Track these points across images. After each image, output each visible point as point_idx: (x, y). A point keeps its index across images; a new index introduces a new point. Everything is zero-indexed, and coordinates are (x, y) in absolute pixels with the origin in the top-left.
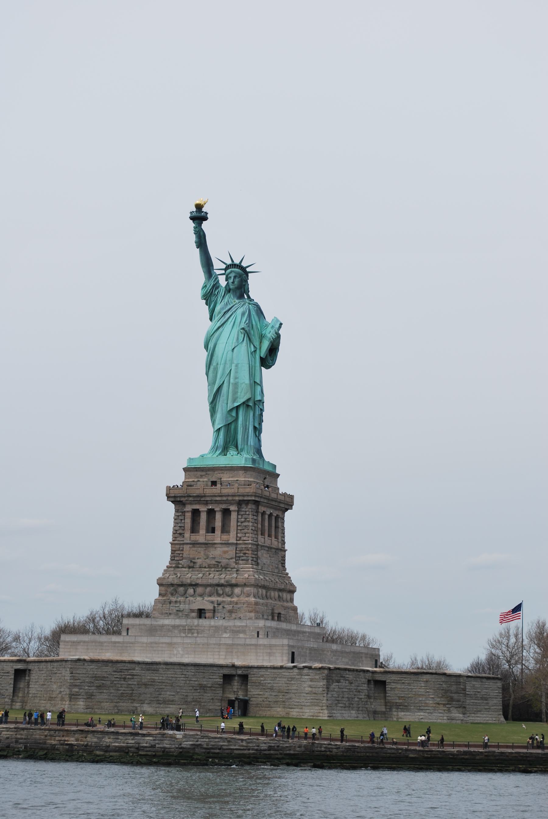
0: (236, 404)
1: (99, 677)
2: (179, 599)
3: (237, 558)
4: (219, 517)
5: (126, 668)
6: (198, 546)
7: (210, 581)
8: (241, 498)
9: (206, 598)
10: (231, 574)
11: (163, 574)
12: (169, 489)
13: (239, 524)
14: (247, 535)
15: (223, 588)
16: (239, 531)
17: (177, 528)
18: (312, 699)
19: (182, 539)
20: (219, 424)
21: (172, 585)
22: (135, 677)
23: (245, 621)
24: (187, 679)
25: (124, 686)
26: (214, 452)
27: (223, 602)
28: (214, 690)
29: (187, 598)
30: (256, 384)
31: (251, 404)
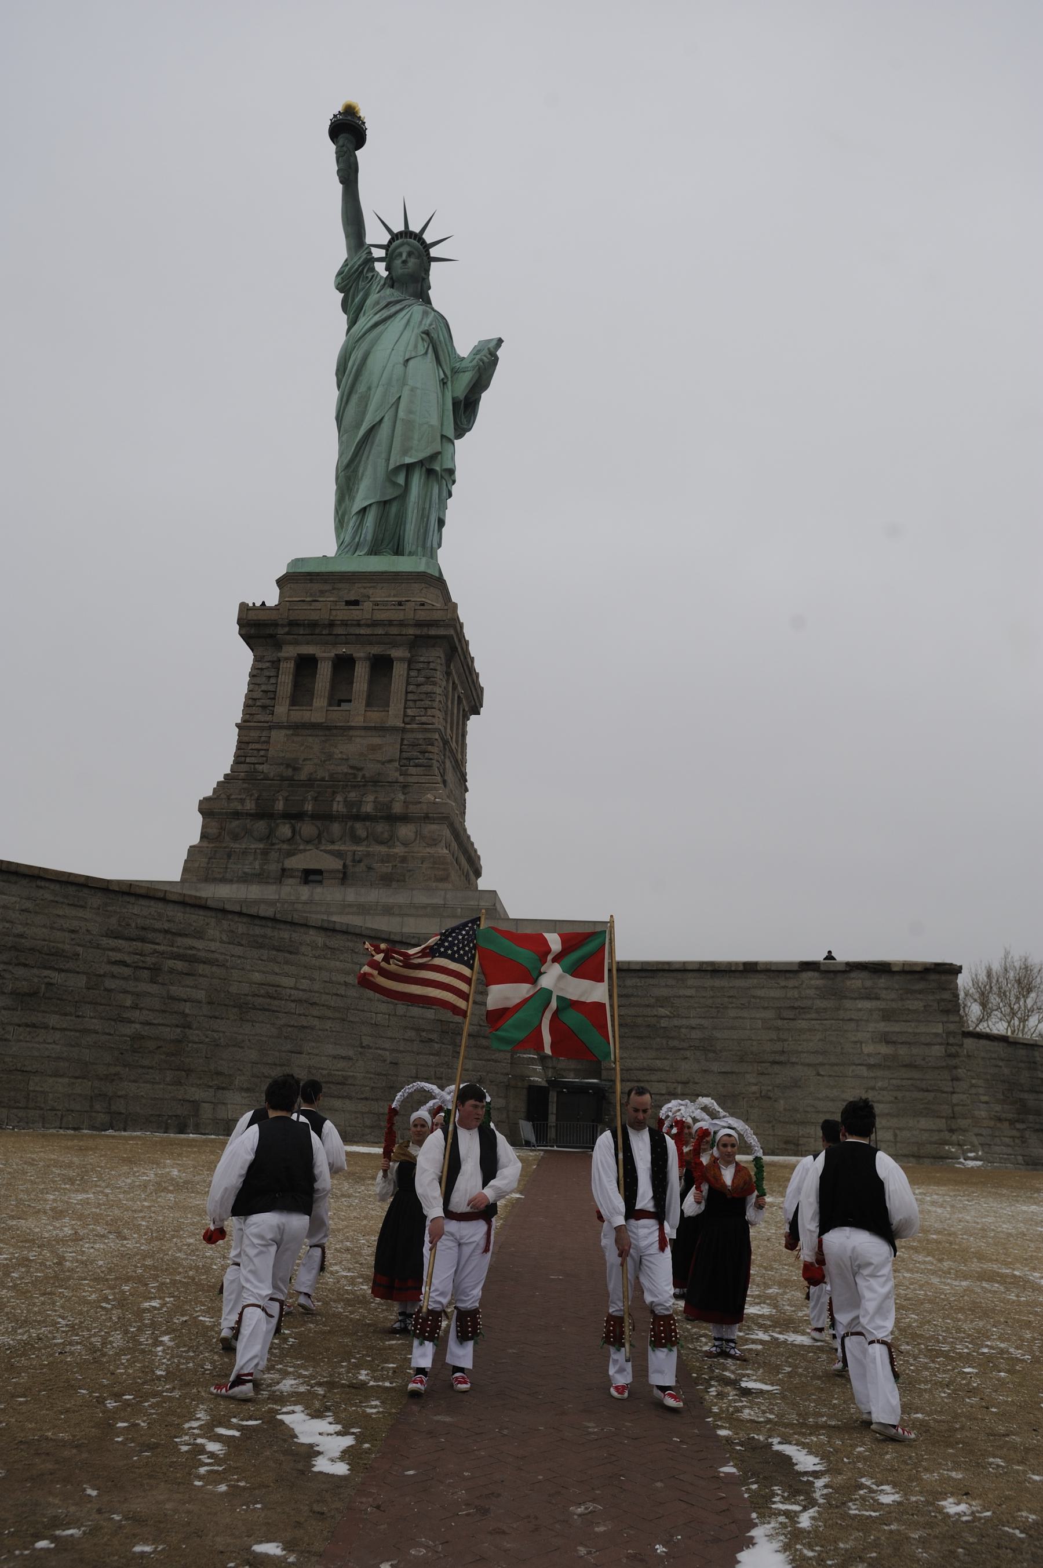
0: (408, 460)
1: (32, 950)
3: (405, 761)
4: (361, 672)
5: (166, 926)
12: (244, 607)
13: (411, 688)
14: (430, 712)
15: (368, 823)
16: (410, 704)
17: (257, 694)
18: (899, 1088)
19: (269, 718)
20: (365, 499)
22: (201, 968)
23: (443, 893)
26: (350, 553)
27: (368, 855)
28: (487, 1048)
30: (444, 440)
31: (438, 468)
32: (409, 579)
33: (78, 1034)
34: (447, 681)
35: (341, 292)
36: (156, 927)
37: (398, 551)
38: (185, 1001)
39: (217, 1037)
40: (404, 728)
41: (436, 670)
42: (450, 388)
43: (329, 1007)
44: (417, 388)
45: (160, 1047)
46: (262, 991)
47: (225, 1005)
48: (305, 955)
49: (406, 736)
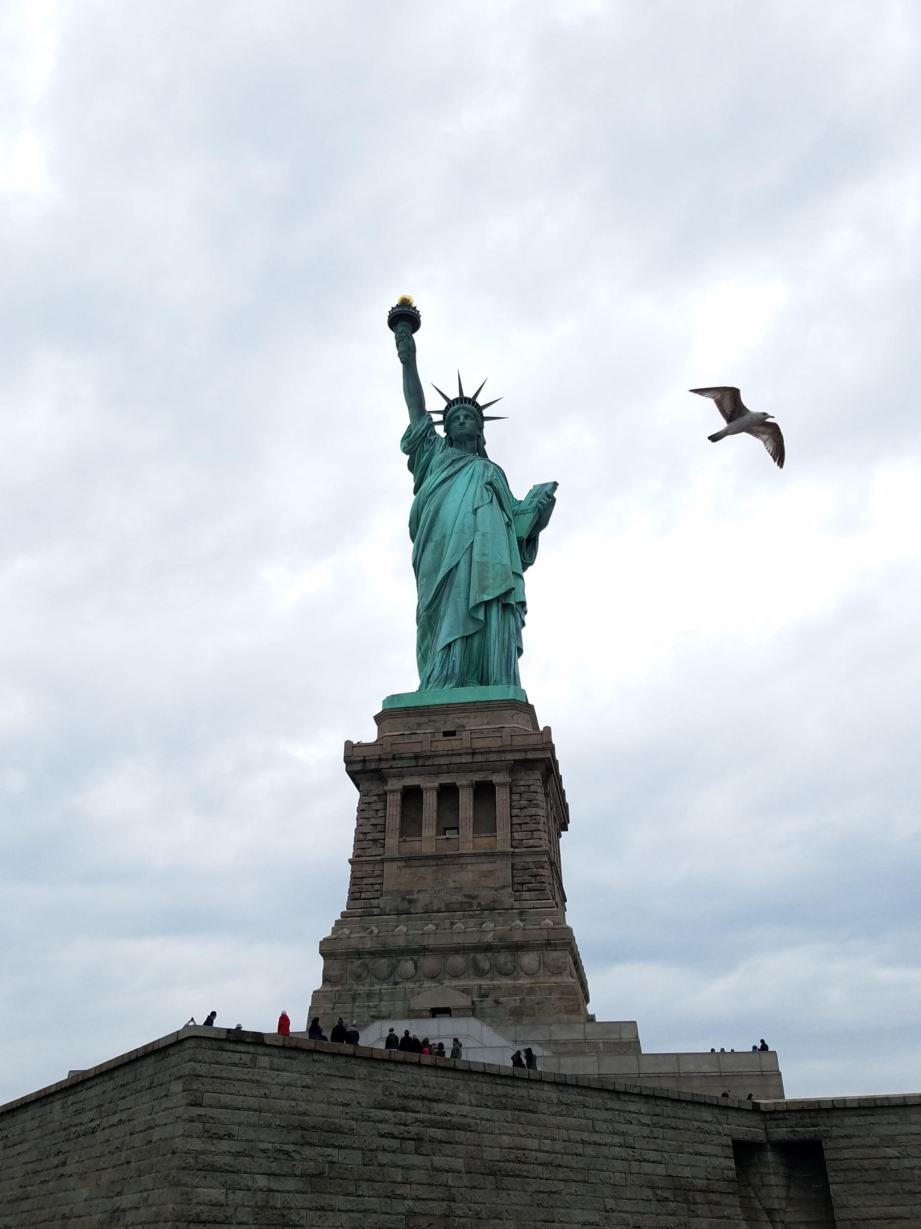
0: (486, 598)
2: (377, 987)
3: (517, 887)
4: (466, 799)
5: (424, 1092)
6: (418, 863)
7: (457, 940)
8: (519, 756)
9: (447, 983)
10: (506, 920)
11: (334, 930)
13: (515, 812)
15: (489, 954)
16: (516, 827)
19: (381, 851)
21: (358, 954)
22: (459, 1135)
24: (630, 1151)
25: (415, 1175)
29: (396, 984)
31: (513, 603)
32: (501, 707)
33: (360, 1215)
34: (547, 804)
35: (406, 453)
36: (415, 1094)
37: (484, 680)
38: (448, 1172)
39: (479, 1209)
40: (513, 852)
41: (536, 792)
42: (514, 528)
43: (571, 1168)
44: (487, 533)
45: (430, 1224)
46: (512, 1156)
47: (483, 1174)
48: (543, 1113)
49: (518, 860)
